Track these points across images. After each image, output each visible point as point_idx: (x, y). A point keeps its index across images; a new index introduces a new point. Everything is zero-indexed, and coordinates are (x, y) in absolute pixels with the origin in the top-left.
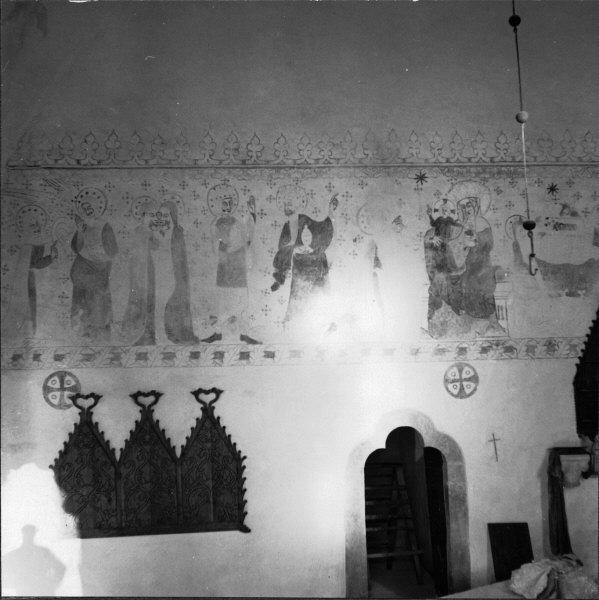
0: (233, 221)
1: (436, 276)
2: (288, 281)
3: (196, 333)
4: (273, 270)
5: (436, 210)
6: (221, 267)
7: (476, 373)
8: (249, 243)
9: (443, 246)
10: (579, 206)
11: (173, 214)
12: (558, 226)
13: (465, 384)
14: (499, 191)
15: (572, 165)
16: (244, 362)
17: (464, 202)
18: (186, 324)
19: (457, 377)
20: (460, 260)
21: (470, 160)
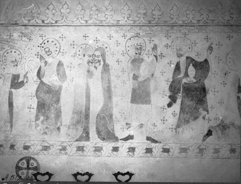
0: (142, 60)
2: (179, 101)
4: (168, 94)
6: (134, 91)
8: (153, 75)
11: (103, 55)
16: (149, 155)
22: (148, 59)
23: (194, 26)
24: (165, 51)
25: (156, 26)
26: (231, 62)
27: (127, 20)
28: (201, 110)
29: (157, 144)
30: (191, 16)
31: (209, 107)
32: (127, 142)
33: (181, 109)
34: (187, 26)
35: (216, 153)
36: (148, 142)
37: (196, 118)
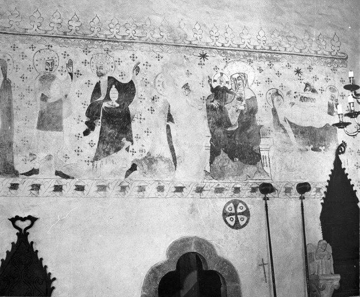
0: (54, 77)
1: (216, 131)
2: (98, 128)
3: (17, 168)
4: (85, 119)
5: (215, 81)
6: (42, 114)
7: (247, 209)
8: (66, 96)
9: (221, 107)
10: (316, 85)
12: (303, 99)
13: (239, 217)
14: (261, 70)
15: (310, 56)
16: (58, 193)
17: (236, 76)
18: (9, 159)
19: (233, 211)
20: (234, 120)
21: (239, 46)
22: (61, 77)
23: (118, 42)
24: (82, 68)
25: (72, 38)
26: (161, 86)
27: (37, 30)
28: (124, 140)
29: (69, 180)
30: (115, 31)
31: (134, 138)
32: (30, 177)
33: (100, 138)
34: (109, 41)
35: (141, 191)
36: (58, 177)
37: (118, 149)
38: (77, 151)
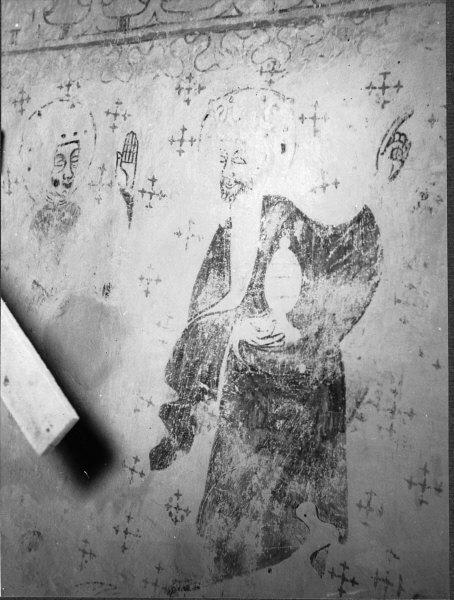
25: (145, 39)
38: (122, 529)
